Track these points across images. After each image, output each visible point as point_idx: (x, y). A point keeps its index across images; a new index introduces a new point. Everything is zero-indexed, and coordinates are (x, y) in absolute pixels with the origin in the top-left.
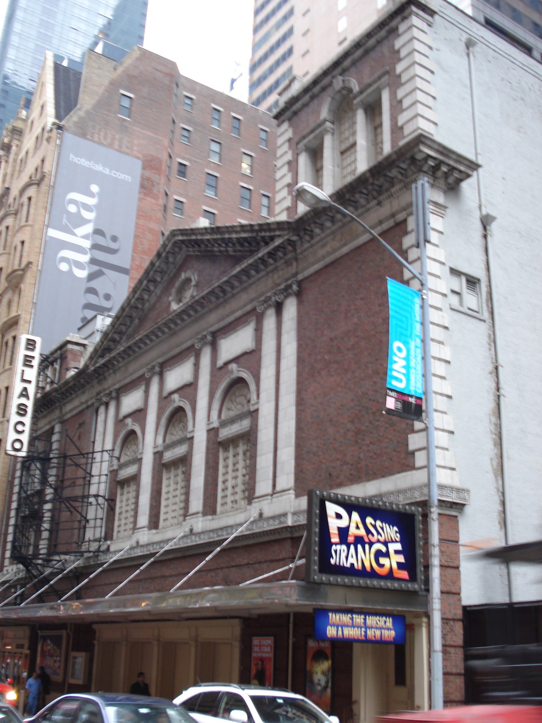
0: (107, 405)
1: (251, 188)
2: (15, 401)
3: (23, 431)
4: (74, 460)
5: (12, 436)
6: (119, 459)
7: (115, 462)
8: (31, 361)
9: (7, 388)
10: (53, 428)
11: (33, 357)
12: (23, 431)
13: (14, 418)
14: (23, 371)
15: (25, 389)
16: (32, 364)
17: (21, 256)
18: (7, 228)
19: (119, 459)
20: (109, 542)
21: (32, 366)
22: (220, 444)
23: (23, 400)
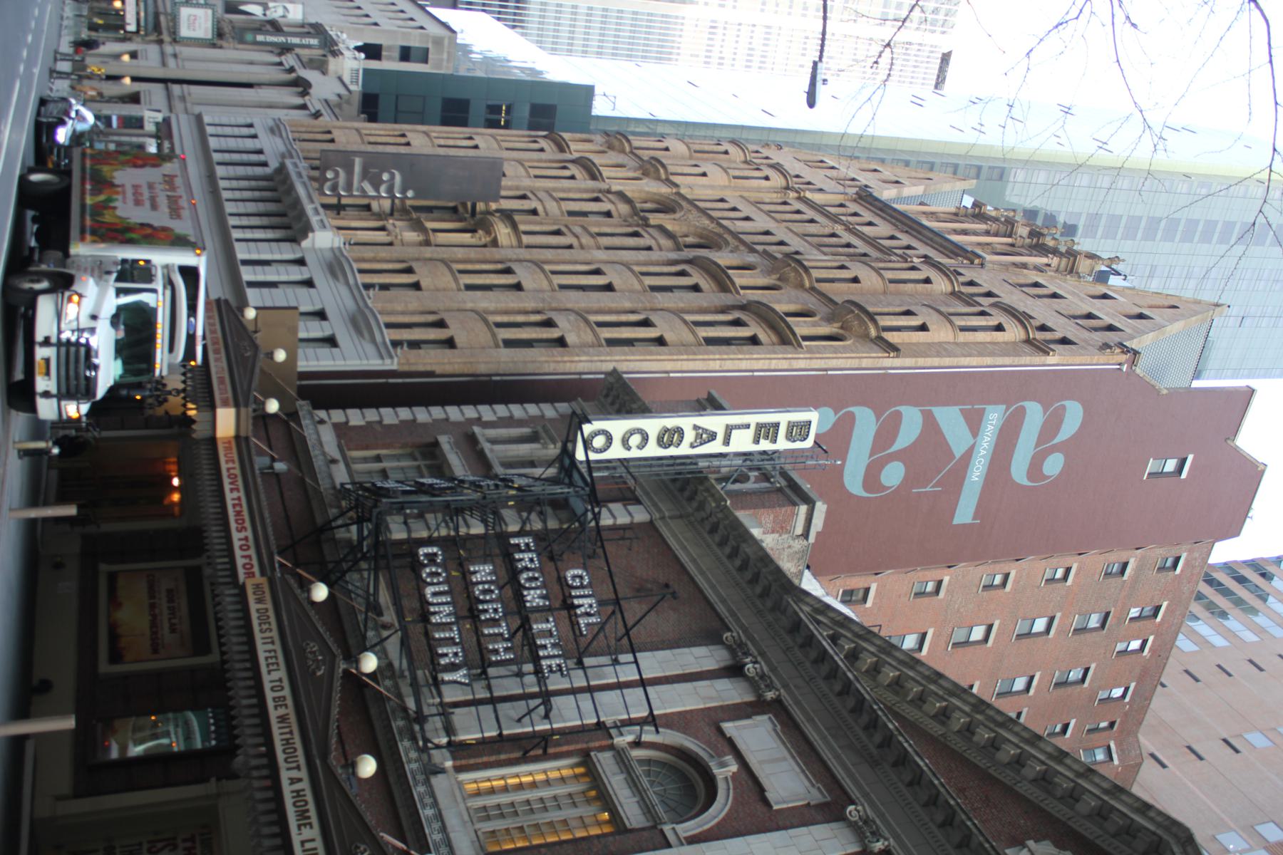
0: (734, 671)
1: (1032, 692)
2: (686, 423)
3: (629, 448)
4: (612, 621)
5: (617, 427)
6: (637, 744)
7: (630, 738)
8: (766, 437)
9: (660, 341)
10: (638, 502)
11: (774, 441)
12: (629, 448)
13: (653, 426)
14: (748, 426)
15: (713, 436)
16: (762, 441)
17: (898, 329)
18: (927, 281)
19: (637, 744)
20: (449, 764)
21: (756, 441)
22: (588, 755)
23: (689, 436)
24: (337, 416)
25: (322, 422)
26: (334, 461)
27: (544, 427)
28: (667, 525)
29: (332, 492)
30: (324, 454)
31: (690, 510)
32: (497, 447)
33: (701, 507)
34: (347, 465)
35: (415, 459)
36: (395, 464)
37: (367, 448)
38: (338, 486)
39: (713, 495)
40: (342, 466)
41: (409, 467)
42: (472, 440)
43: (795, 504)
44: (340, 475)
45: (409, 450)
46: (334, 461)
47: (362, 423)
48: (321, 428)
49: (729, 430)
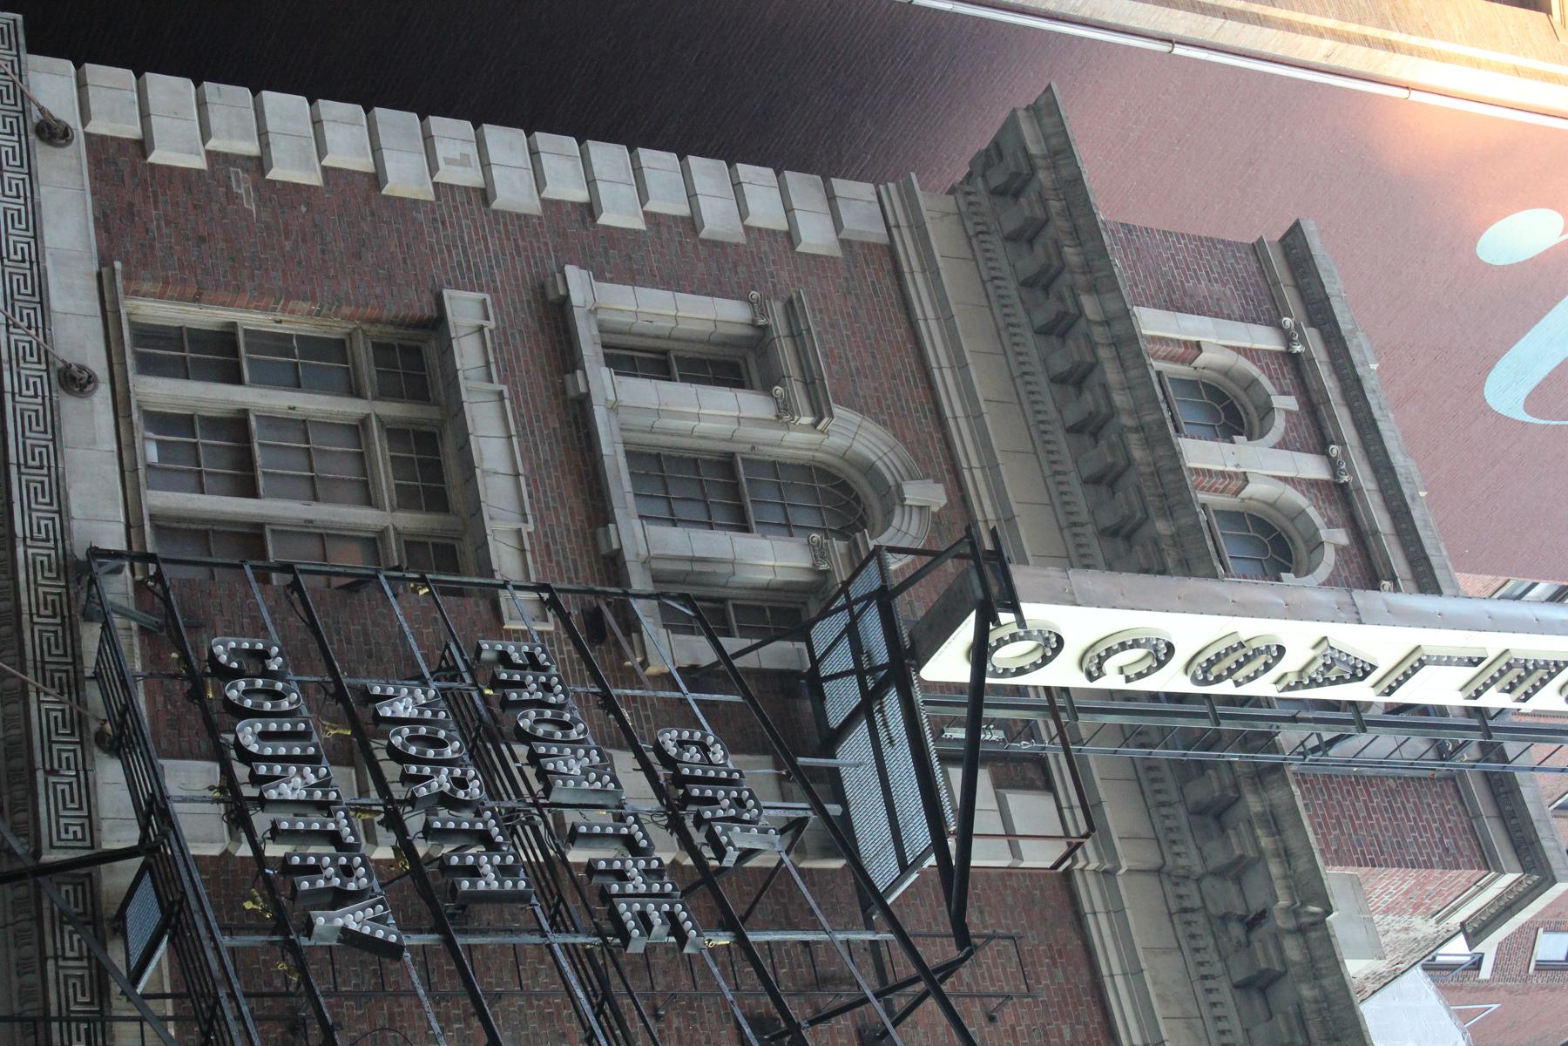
14: (1472, 663)
15: (1360, 672)
24: (112, 99)
25: (52, 133)
26: (74, 381)
27: (790, 306)
28: (1116, 911)
29: (50, 586)
30: (46, 357)
31: (1198, 869)
32: (642, 392)
33: (1236, 871)
34: (121, 404)
35: (355, 392)
36: (278, 400)
37: (197, 299)
38: (81, 555)
39: (1286, 855)
40: (102, 397)
41: (327, 426)
42: (556, 316)
43: (1488, 862)
44: (99, 520)
45: (334, 328)
46: (74, 381)
47: (199, 163)
48: (48, 160)
49: (1415, 663)
